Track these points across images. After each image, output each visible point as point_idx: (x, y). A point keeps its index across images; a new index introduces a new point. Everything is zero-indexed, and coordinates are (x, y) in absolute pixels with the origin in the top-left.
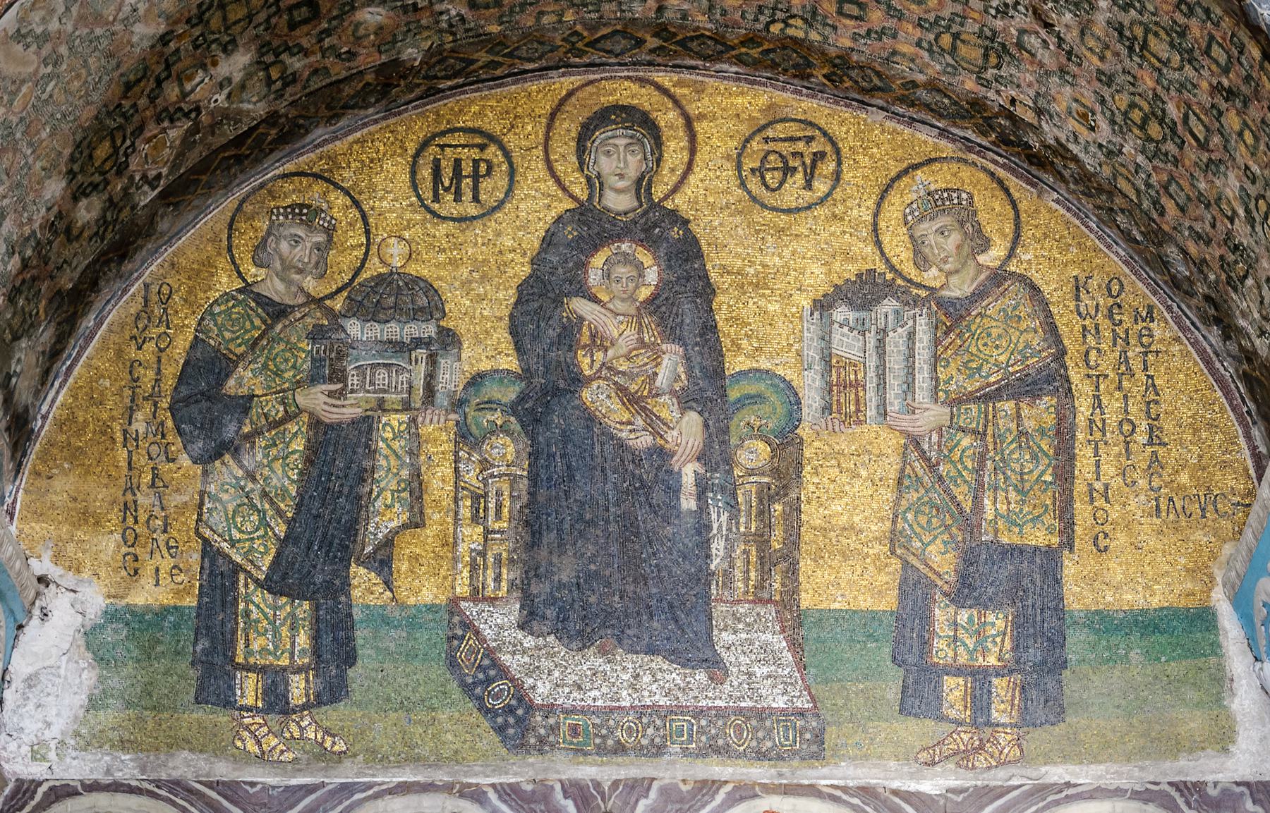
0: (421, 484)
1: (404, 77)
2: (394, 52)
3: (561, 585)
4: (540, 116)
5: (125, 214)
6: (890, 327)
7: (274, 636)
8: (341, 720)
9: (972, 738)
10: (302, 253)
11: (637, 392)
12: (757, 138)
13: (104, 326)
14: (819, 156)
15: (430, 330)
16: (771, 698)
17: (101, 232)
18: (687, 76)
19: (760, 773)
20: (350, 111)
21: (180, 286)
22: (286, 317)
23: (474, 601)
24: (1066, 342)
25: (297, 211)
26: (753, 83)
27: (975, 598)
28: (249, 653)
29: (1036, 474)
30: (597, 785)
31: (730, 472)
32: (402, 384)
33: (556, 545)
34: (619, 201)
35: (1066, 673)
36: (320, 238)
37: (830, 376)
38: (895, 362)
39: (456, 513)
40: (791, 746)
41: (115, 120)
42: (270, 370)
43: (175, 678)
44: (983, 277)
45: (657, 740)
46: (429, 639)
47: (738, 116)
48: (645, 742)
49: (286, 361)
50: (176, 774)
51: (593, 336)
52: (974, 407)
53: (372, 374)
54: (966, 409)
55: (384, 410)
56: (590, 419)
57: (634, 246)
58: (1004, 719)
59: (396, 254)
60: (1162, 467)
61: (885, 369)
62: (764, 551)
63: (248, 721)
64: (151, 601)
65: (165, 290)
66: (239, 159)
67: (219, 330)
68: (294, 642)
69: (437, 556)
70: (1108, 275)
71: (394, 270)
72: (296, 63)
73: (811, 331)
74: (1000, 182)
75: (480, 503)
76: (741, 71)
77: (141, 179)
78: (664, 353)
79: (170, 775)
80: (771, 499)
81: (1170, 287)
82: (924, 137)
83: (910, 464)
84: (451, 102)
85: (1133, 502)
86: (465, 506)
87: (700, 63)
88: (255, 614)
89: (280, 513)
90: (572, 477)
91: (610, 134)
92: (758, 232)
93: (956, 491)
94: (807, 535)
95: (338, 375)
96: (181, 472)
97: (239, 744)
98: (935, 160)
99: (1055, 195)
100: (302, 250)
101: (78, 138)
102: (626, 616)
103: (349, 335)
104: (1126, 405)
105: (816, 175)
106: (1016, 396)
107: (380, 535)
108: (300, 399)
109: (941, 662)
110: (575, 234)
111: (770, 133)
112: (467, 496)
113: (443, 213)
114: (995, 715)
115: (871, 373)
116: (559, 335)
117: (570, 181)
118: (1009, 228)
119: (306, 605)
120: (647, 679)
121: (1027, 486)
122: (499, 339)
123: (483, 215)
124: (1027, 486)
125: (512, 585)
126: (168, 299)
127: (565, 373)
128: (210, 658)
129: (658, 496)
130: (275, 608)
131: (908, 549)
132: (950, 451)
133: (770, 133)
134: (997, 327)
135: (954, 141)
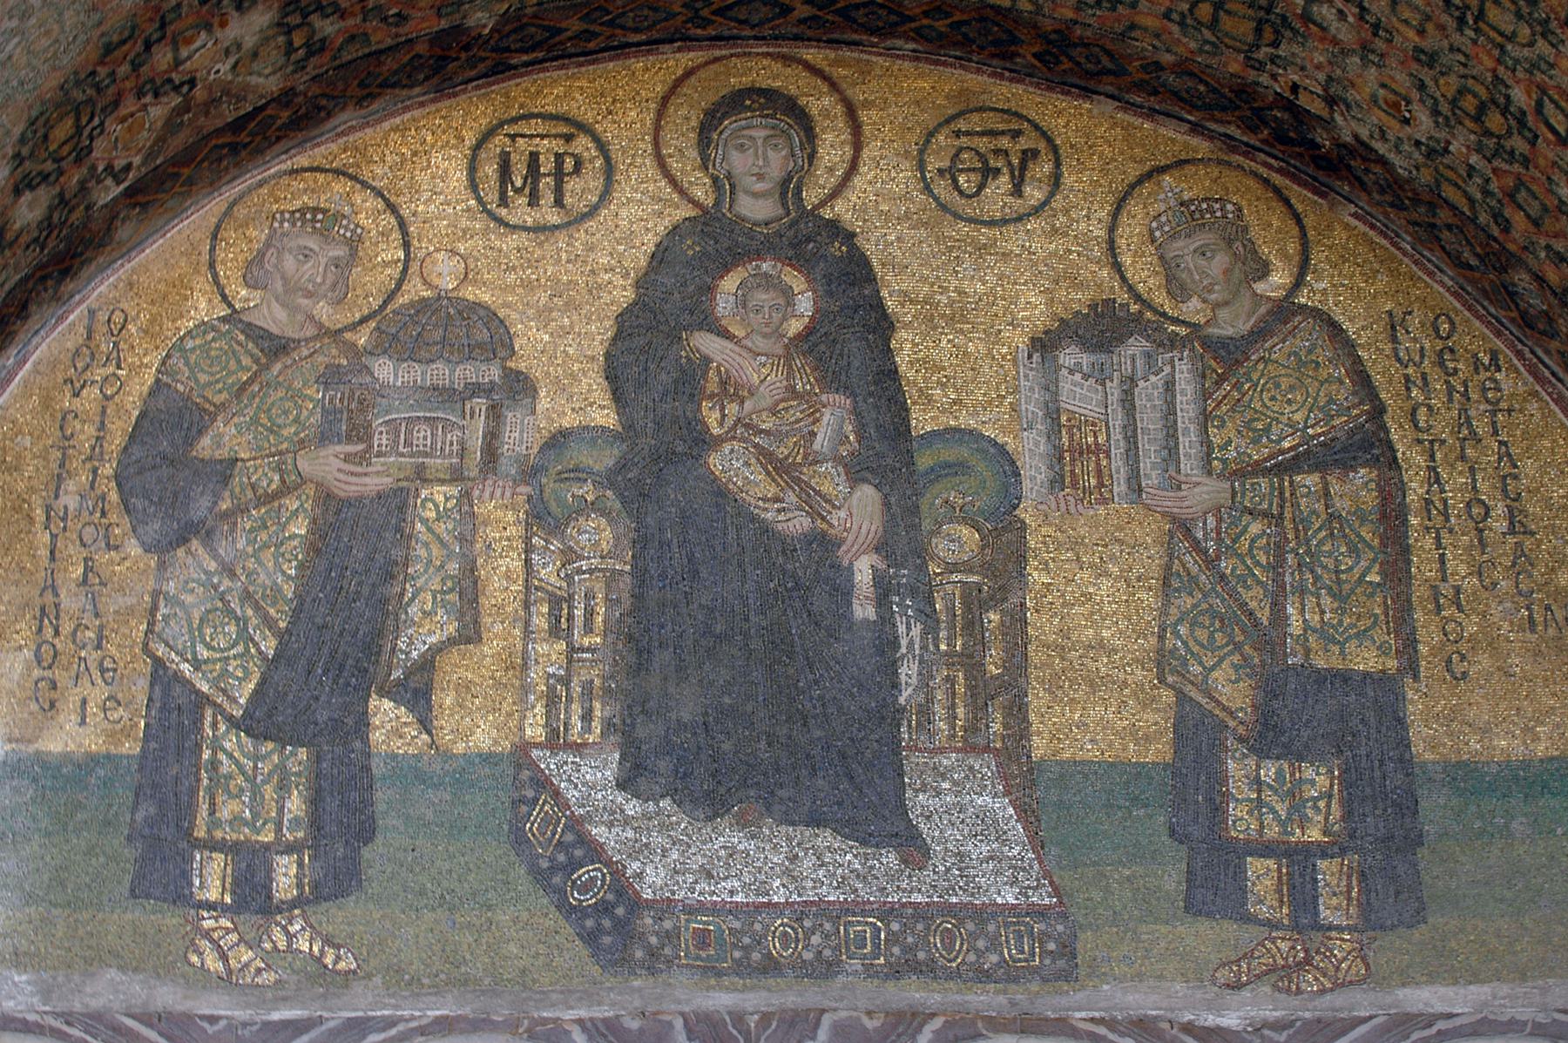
0: (476, 583)
1: (467, 48)
2: (457, 16)
3: (681, 726)
4: (647, 101)
5: (77, 216)
6: (1139, 374)
7: (253, 799)
8: (349, 924)
9: (1293, 948)
10: (315, 271)
11: (787, 458)
12: (945, 131)
13: (28, 366)
14: (1029, 156)
15: (493, 373)
16: (993, 889)
17: (42, 238)
18: (847, 53)
19: (984, 999)
20: (389, 91)
21: (139, 312)
22: (288, 354)
23: (551, 749)
24: (1383, 396)
25: (308, 216)
26: (937, 63)
27: (1284, 746)
28: (214, 823)
29: (1357, 572)
30: (739, 1018)
31: (923, 567)
32: (451, 444)
33: (672, 668)
34: (756, 208)
35: (1423, 852)
36: (340, 252)
37: (1060, 440)
38: (1149, 421)
39: (527, 623)
40: (1026, 960)
41: (84, 91)
42: (262, 425)
43: (102, 859)
44: (1263, 310)
45: (827, 953)
46: (485, 804)
47: (918, 103)
48: (808, 956)
49: (286, 413)
50: (96, 1004)
51: (724, 383)
52: (1264, 483)
53: (409, 432)
54: (1252, 484)
55: (425, 481)
56: (720, 493)
57: (779, 265)
58: (1337, 919)
59: (445, 273)
60: (1531, 564)
61: (1135, 430)
62: (975, 679)
63: (208, 924)
64: (72, 747)
65: (118, 318)
66: (234, 148)
67: (191, 370)
68: (283, 807)
69: (498, 684)
70: (1433, 311)
71: (443, 293)
72: (327, 27)
73: (1030, 381)
74: (1277, 191)
75: (562, 609)
76: (920, 48)
77: (105, 170)
78: (824, 406)
79: (87, 1006)
80: (984, 606)
81: (1519, 326)
82: (1171, 134)
83: (1178, 558)
84: (525, 82)
85: (1496, 610)
86: (539, 613)
87: (865, 37)
88: (226, 766)
89: (269, 622)
90: (695, 574)
91: (744, 122)
92: (950, 250)
93: (1246, 595)
94: (1035, 655)
95: (360, 432)
96: (127, 564)
97: (194, 959)
98: (1187, 162)
99: (1352, 208)
100: (313, 266)
101: (34, 113)
102: (778, 770)
103: (378, 379)
104: (1474, 481)
105: (1027, 180)
106: (1320, 467)
107: (415, 654)
108: (303, 465)
109: (1241, 836)
110: (698, 249)
111: (962, 125)
112: (543, 599)
113: (513, 221)
114: (1325, 914)
115: (1117, 435)
116: (676, 381)
117: (690, 182)
118: (1292, 247)
119: (303, 754)
120: (808, 862)
121: (1346, 587)
122: (590, 385)
123: (569, 224)
124: (1346, 587)
125: (608, 726)
126: (121, 330)
127: (685, 431)
128: (155, 831)
129: (820, 601)
130: (256, 758)
131: (1184, 676)
132: (1234, 541)
133: (962, 125)
134: (1286, 375)
135: (1211, 138)
